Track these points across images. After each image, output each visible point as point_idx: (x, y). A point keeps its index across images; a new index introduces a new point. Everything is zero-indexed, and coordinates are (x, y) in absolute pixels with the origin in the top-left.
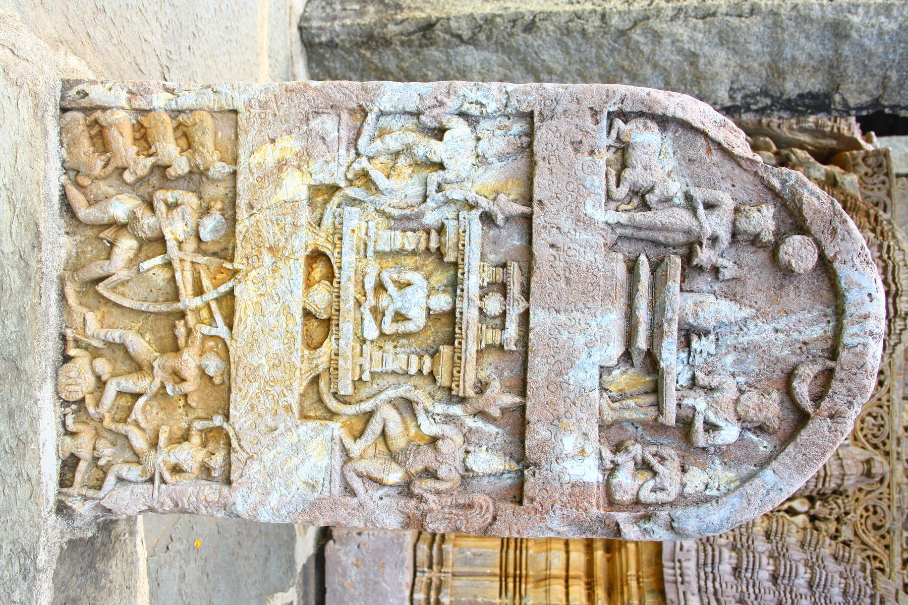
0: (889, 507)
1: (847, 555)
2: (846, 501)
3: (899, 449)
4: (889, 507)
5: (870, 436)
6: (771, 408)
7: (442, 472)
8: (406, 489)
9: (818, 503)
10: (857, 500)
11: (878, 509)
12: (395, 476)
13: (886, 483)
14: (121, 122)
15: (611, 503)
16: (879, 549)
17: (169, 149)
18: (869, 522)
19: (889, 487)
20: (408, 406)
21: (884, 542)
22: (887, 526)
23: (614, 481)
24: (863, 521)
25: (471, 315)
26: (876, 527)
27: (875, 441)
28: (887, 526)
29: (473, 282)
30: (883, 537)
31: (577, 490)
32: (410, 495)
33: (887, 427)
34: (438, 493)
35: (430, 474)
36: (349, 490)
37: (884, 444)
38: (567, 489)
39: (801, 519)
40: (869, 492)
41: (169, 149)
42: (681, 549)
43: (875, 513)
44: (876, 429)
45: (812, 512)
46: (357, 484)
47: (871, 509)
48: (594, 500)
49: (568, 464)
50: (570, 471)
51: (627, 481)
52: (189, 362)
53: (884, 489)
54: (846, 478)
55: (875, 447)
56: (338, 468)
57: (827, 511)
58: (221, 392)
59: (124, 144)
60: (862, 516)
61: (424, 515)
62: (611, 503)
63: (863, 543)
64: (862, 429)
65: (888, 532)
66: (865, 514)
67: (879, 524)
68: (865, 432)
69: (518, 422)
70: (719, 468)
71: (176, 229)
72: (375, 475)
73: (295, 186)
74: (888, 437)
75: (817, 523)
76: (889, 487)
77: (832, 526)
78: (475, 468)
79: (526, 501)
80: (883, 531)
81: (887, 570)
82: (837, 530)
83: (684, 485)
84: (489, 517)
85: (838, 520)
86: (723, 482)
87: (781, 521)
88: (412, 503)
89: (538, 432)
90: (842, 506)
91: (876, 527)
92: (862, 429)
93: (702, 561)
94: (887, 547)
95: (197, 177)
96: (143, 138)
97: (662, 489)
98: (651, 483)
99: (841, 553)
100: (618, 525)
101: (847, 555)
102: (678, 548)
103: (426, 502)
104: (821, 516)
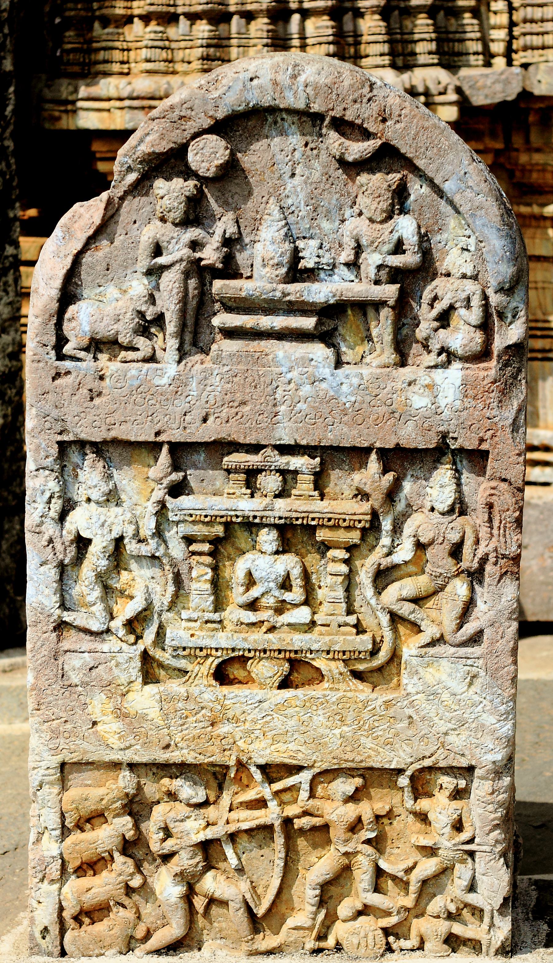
6: (378, 182)
7: (455, 537)
8: (476, 576)
12: (460, 588)
14: (78, 891)
15: (484, 354)
17: (105, 836)
20: (383, 577)
23: (460, 352)
25: (282, 507)
29: (248, 506)
31: (471, 393)
32: (481, 570)
34: (477, 542)
35: (456, 552)
36: (476, 639)
38: (468, 403)
41: (105, 836)
46: (469, 628)
48: (482, 374)
49: (442, 402)
50: (450, 400)
51: (462, 336)
52: (337, 811)
56: (453, 650)
58: (373, 778)
59: (101, 886)
61: (504, 556)
62: (484, 354)
69: (398, 459)
70: (445, 236)
71: (194, 830)
72: (458, 610)
73: (145, 699)
78: (450, 501)
79: (484, 447)
83: (464, 276)
84: (504, 486)
86: (461, 232)
88: (489, 568)
89: (410, 436)
95: (136, 807)
96: (92, 866)
97: (468, 300)
98: (462, 312)
100: (509, 347)
103: (487, 555)
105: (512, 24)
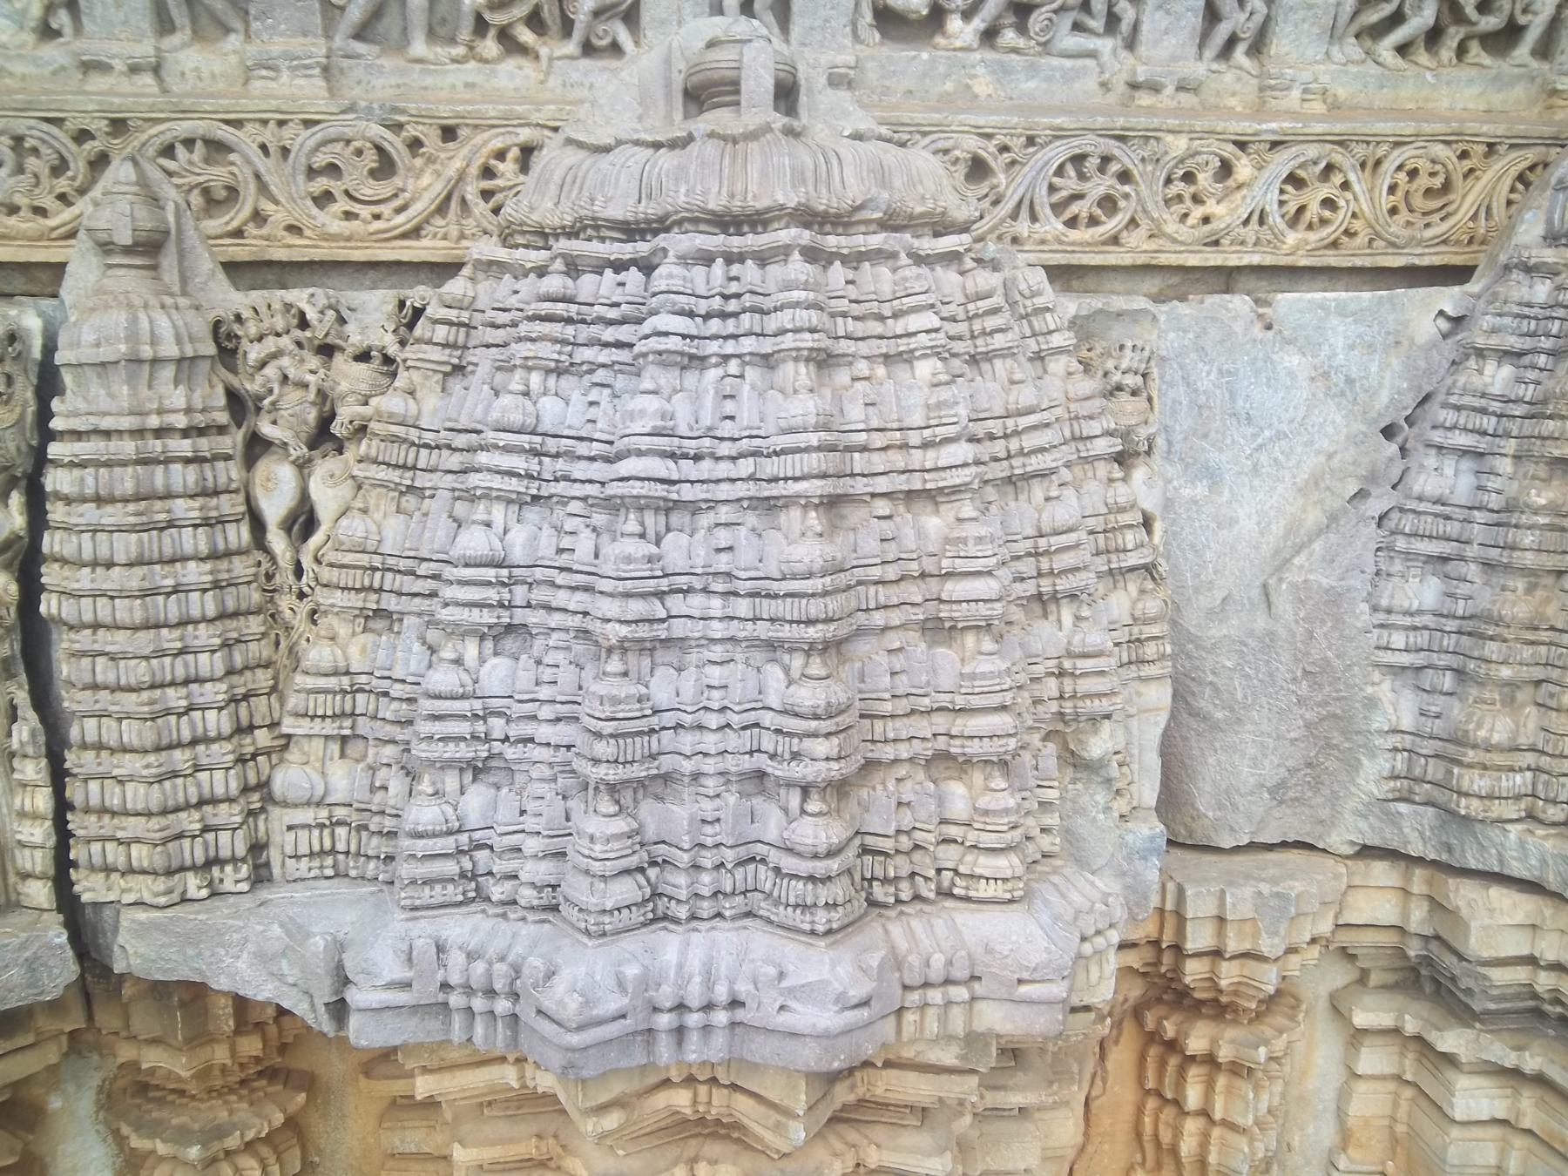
0: (308, 123)
1: (441, 333)
2: (253, 330)
3: (119, 65)
4: (308, 123)
5: (62, 184)
9: (266, 429)
10: (293, 229)
11: (320, 160)
13: (225, 133)
16: (456, 159)
18: (371, 189)
19: (237, 124)
21: (432, 140)
22: (376, 130)
24: (365, 212)
26: (385, 166)
27: (78, 167)
28: (376, 130)
30: (415, 144)
33: (20, 126)
37: (83, 136)
39: (326, 499)
40: (263, 188)
42: (406, 985)
43: (333, 169)
44: (32, 163)
45: (299, 450)
47: (321, 184)
53: (246, 140)
54: (147, 352)
55: (100, 162)
57: (293, 396)
60: (349, 216)
63: (442, 209)
64: (40, 211)
65: (397, 127)
66: (343, 204)
67: (371, 160)
68: (48, 202)
74: (57, 122)
75: (336, 429)
76: (237, 124)
77: (349, 376)
80: (395, 145)
81: (525, 135)
82: (363, 357)
85: (326, 351)
87: (326, 574)
90: (270, 344)
91: (385, 166)
92: (40, 211)
93: (453, 893)
94: (449, 133)
99: (436, 354)
101: (441, 333)
102: (402, 998)
104: (312, 415)
105: (62, 806)
